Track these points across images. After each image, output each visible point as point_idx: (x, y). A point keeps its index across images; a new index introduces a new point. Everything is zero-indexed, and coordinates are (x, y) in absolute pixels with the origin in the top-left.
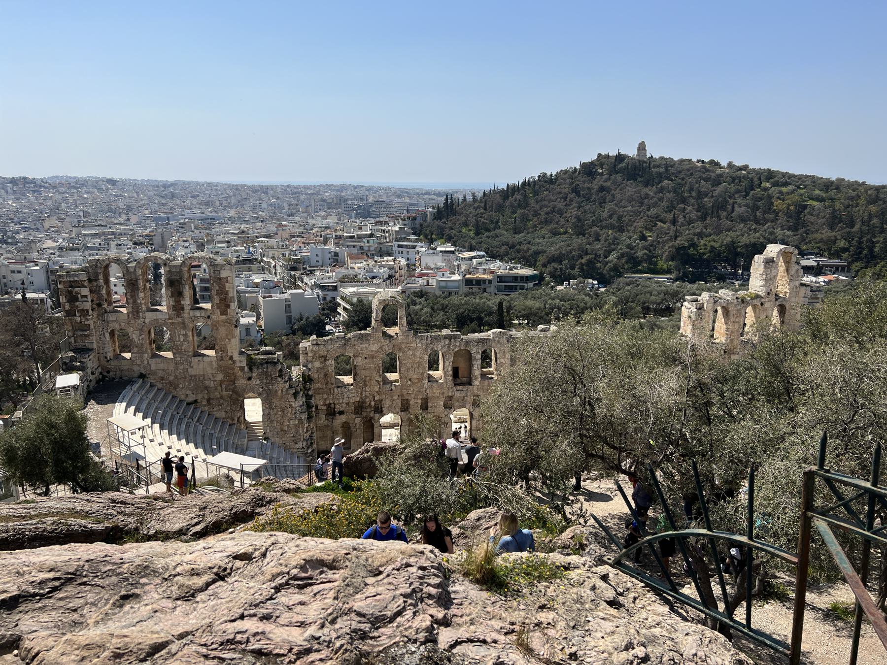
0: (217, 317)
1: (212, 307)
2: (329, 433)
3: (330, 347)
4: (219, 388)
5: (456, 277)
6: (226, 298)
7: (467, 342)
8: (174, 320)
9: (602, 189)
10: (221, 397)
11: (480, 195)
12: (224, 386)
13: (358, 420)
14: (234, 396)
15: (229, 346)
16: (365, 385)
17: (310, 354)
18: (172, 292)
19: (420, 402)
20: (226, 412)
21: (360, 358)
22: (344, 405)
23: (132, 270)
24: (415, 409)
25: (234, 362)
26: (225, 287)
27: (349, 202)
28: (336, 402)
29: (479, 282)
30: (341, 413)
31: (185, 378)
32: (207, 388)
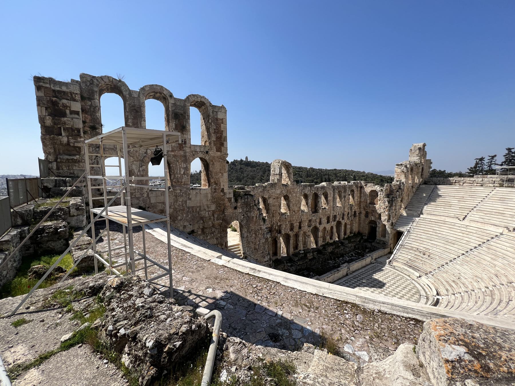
3: (256, 192)
4: (212, 217)
6: (221, 137)
8: (177, 153)
9: (241, 168)
10: (213, 226)
12: (216, 216)
14: (224, 224)
15: (221, 180)
16: (273, 216)
18: (176, 125)
19: (298, 224)
20: (217, 239)
23: (136, 96)
24: (296, 229)
25: (225, 194)
31: (184, 210)
32: (202, 218)
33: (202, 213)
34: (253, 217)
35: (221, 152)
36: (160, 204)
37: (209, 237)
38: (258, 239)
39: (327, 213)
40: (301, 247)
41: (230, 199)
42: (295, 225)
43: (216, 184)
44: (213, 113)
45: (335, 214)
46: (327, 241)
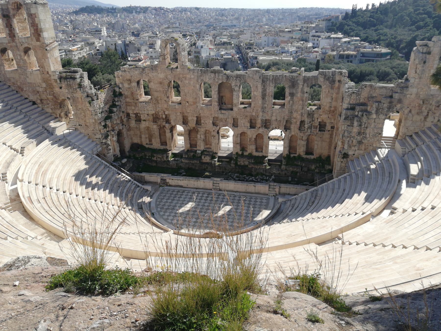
0: (35, 43)
1: (31, 35)
2: (138, 132)
4: (45, 93)
5: (335, 53)
7: (228, 77)
11: (377, 5)
12: (48, 92)
13: (155, 127)
14: (54, 99)
15: (45, 64)
17: (121, 78)
18: (6, 24)
19: (195, 119)
20: (52, 109)
21: (152, 83)
22: (146, 116)
25: (50, 76)
26: (35, 20)
27: (311, 17)
28: (141, 112)
29: (348, 56)
30: (144, 120)
32: (38, 92)
33: (38, 88)
34: (78, 98)
35: (40, 41)
36: (12, 79)
37: (45, 106)
38: (87, 118)
39: (248, 114)
40: (201, 147)
41: (56, 81)
42: (189, 118)
43: (42, 67)
44: (27, 10)
45: (267, 118)
46: (249, 151)
